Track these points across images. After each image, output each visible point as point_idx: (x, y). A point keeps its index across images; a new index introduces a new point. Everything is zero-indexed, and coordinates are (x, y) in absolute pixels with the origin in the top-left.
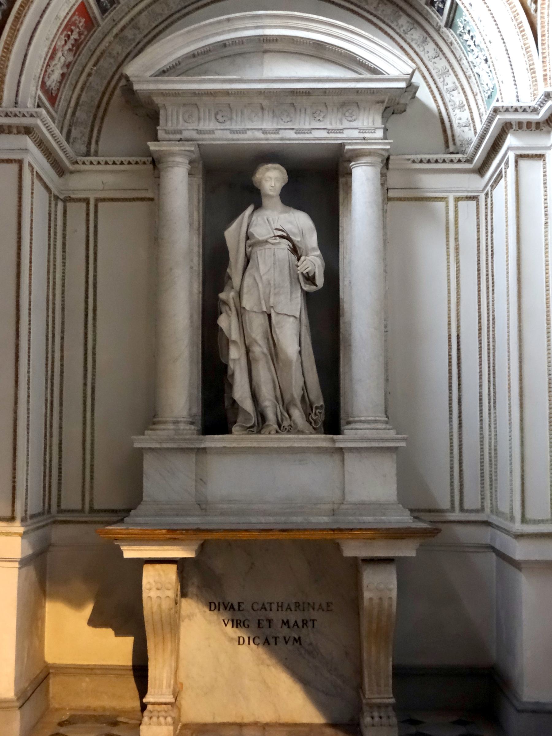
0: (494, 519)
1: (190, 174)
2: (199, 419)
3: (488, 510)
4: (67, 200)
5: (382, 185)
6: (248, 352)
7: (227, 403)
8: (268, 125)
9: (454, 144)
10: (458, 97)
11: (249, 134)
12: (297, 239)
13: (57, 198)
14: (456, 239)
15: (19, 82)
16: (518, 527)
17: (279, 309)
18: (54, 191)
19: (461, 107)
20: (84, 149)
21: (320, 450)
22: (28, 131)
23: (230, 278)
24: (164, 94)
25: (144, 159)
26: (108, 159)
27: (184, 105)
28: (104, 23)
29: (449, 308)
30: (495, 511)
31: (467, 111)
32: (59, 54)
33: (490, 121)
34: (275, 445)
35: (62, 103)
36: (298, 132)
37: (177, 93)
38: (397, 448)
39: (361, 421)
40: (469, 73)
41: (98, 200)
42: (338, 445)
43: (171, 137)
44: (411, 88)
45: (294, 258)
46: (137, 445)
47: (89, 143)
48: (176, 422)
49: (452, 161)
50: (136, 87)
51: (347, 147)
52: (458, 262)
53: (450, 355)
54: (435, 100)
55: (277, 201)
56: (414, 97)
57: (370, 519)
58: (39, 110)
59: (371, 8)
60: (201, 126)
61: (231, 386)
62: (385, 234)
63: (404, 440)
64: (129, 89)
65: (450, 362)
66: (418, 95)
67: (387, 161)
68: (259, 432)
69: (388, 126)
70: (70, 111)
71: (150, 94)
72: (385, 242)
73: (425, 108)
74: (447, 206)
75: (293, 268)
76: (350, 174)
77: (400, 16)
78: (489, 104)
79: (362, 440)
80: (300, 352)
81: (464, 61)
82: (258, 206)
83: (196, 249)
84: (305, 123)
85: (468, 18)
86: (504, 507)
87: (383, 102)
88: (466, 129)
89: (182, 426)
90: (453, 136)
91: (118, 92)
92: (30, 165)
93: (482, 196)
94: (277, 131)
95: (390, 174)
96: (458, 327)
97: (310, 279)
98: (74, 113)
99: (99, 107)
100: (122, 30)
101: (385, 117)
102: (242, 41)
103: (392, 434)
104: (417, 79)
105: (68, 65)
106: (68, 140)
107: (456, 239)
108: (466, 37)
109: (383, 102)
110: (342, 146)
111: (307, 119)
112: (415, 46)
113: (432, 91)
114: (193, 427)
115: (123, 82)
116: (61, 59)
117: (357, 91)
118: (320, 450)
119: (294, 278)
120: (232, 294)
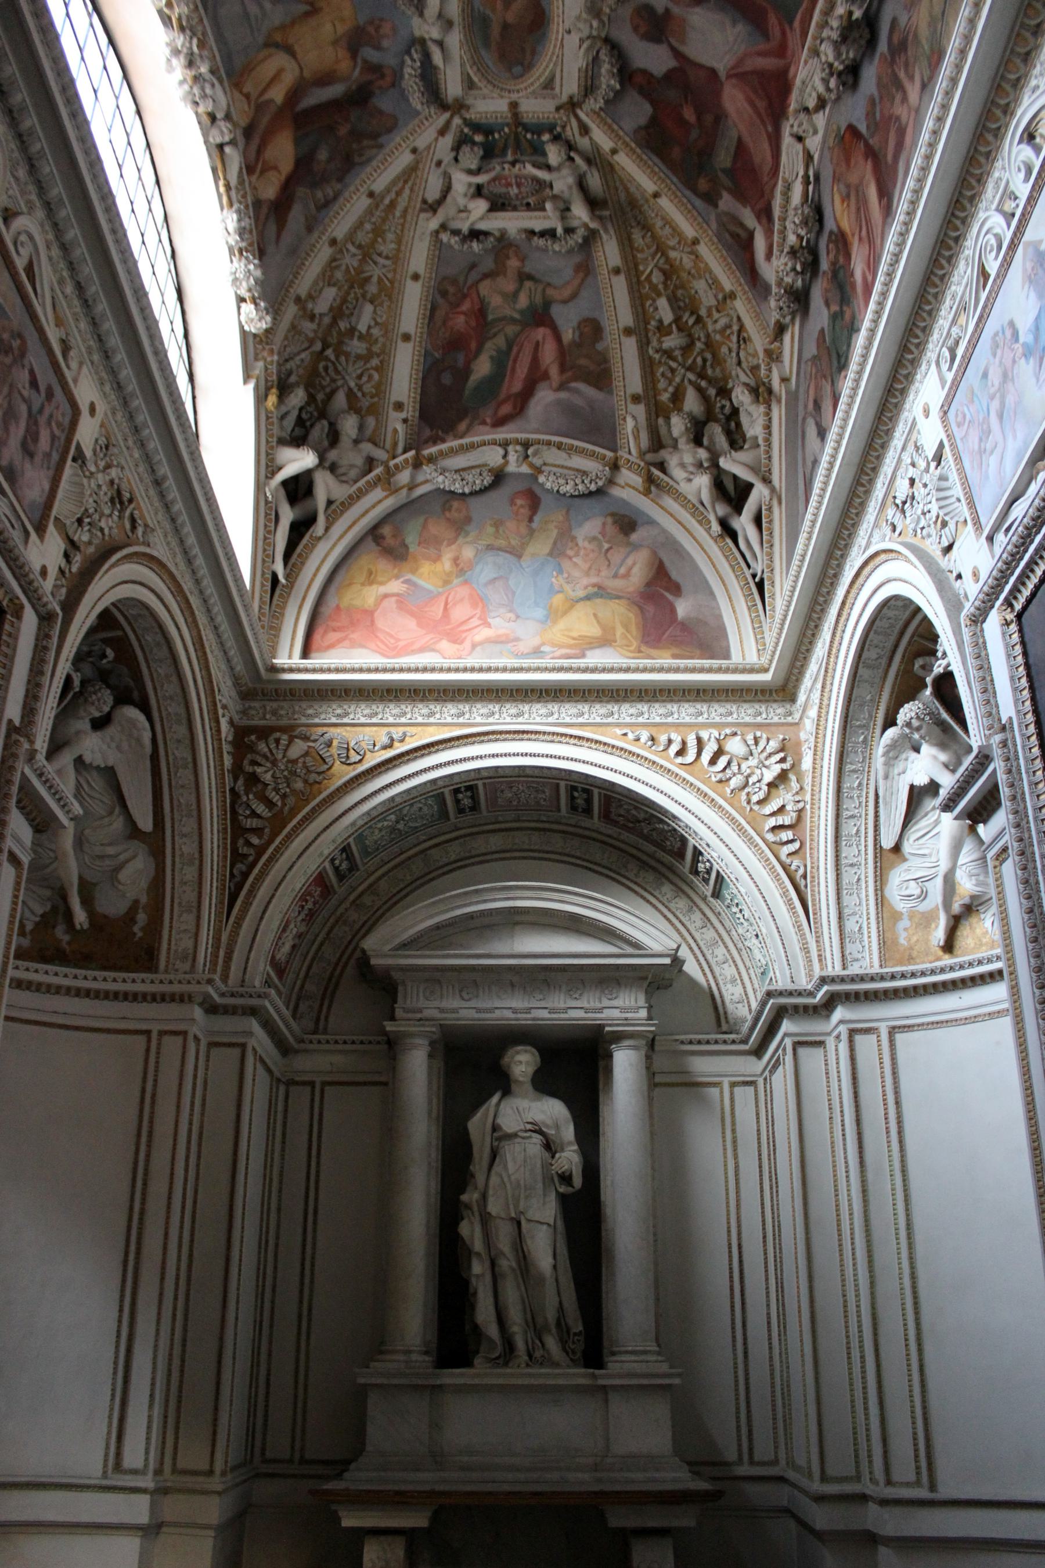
0: (791, 1475)
1: (430, 1056)
3: (783, 1462)
4: (291, 1083)
5: (648, 1068)
6: (493, 1264)
9: (727, 1022)
10: (729, 971)
11: (498, 1014)
13: (279, 1080)
14: (734, 1131)
15: (248, 959)
16: (817, 1487)
17: (530, 1215)
18: (277, 1074)
19: (733, 981)
20: (311, 1026)
22: (253, 1012)
23: (473, 1176)
25: (380, 1038)
26: (337, 1037)
27: (427, 980)
28: (341, 890)
29: (728, 1211)
30: (791, 1463)
31: (740, 986)
32: (292, 926)
33: (763, 1004)
34: (526, 1381)
35: (290, 977)
36: (552, 1011)
38: (670, 1386)
39: (627, 1352)
40: (740, 945)
41: (324, 1084)
42: (601, 1382)
43: (410, 1015)
44: (677, 962)
45: (547, 1155)
46: (361, 1381)
47: (318, 1020)
48: (408, 1352)
49: (725, 1042)
50: (373, 962)
51: (607, 1029)
52: (736, 1156)
53: (731, 1269)
54: (705, 974)
55: (529, 1087)
56: (680, 971)
57: (639, 1476)
58: (267, 990)
59: (631, 875)
60: (445, 1004)
61: (473, 1307)
62: (652, 1125)
63: (679, 1375)
64: (364, 961)
65: (731, 1277)
66: (685, 968)
67: (652, 1044)
70: (299, 983)
71: (388, 969)
72: (652, 1134)
73: (692, 982)
74: (722, 1092)
75: (546, 1166)
76: (610, 1056)
77: (662, 884)
78: (763, 981)
80: (555, 1267)
81: (734, 932)
82: (507, 1092)
83: (434, 1142)
85: (735, 891)
86: (801, 1462)
87: (645, 978)
88: (740, 1006)
89: (414, 1357)
90: (725, 1013)
91: (352, 962)
92: (254, 1049)
93: (761, 1081)
94: (528, 1010)
96: (739, 1234)
97: (566, 1178)
98: (302, 986)
99: (330, 979)
100: (360, 896)
101: (649, 995)
102: (491, 912)
103: (664, 1368)
104: (684, 953)
105: (300, 936)
106: (294, 1016)
107: (734, 1131)
108: (734, 909)
109: (646, 978)
110: (601, 1027)
111: (562, 996)
112: (680, 916)
113: (700, 964)
114: (427, 1358)
115: (358, 954)
116: (293, 930)
117: (618, 967)
118: (578, 1389)
119: (548, 1179)
120: (476, 1196)
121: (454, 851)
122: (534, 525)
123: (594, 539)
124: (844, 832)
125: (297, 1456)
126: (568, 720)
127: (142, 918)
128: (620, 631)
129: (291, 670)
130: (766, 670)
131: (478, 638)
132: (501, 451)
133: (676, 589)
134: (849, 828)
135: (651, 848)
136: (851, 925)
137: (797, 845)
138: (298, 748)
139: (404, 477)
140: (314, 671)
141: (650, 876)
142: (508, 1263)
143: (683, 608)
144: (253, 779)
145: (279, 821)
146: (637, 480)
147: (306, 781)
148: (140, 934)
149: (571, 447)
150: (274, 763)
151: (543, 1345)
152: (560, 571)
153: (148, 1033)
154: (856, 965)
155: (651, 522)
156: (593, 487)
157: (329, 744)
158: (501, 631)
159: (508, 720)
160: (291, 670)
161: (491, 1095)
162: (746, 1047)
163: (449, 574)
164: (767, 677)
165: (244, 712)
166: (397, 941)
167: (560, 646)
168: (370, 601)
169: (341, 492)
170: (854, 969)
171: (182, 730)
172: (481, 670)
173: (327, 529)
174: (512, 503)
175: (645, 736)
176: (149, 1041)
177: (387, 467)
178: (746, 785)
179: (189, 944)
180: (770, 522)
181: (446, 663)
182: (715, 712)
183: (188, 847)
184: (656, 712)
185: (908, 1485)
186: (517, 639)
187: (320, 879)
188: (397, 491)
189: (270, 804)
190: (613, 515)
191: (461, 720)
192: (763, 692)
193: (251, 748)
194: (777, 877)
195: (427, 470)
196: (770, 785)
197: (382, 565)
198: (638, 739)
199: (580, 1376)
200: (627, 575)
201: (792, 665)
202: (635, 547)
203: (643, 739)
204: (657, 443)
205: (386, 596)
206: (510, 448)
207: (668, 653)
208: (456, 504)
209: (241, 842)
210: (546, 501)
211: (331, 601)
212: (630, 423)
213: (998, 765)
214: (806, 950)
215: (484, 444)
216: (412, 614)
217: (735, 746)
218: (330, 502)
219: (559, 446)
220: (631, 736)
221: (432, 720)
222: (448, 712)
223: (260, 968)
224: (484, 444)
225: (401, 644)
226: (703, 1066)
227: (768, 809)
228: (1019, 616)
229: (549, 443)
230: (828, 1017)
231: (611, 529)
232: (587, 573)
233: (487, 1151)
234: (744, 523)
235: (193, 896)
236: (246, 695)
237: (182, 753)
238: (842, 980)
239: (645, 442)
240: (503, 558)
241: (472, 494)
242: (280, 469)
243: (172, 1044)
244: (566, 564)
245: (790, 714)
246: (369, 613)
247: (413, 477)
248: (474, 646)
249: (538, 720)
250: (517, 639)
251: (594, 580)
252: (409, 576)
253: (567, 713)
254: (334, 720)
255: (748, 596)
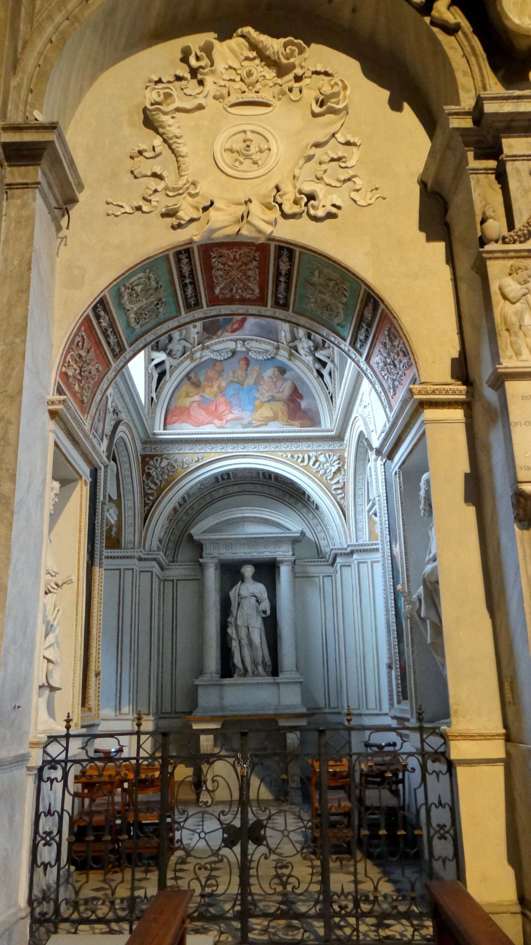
1: (216, 569)
2: (220, 671)
3: (340, 707)
6: (240, 642)
7: (231, 664)
8: (246, 551)
10: (322, 535)
11: (239, 554)
12: (258, 595)
14: (324, 593)
17: (252, 625)
19: (324, 539)
20: (171, 559)
21: (269, 684)
22: (154, 560)
23: (232, 612)
24: (204, 539)
37: (210, 539)
41: (177, 580)
44: (303, 533)
46: (196, 683)
48: (211, 673)
52: (325, 603)
59: (287, 500)
61: (233, 657)
64: (191, 536)
68: (245, 676)
69: (295, 547)
73: (309, 539)
75: (257, 608)
76: (279, 567)
79: (286, 678)
80: (261, 643)
84: (262, 550)
94: (250, 553)
95: (296, 567)
97: (265, 612)
102: (236, 518)
103: (298, 676)
106: (165, 555)
107: (324, 593)
110: (275, 558)
117: (281, 537)
118: (269, 684)
119: (258, 611)
120: (233, 619)
121: (222, 492)
122: (248, 372)
123: (270, 377)
124: (357, 493)
125: (173, 711)
126: (262, 450)
127: (114, 529)
128: (280, 414)
129: (161, 434)
130: (333, 431)
131: (228, 418)
132: (235, 343)
133: (301, 397)
134: (359, 492)
135: (292, 490)
136: (360, 526)
137: (343, 495)
138: (164, 463)
139: (198, 355)
140: (169, 434)
141: (294, 500)
142: (245, 642)
143: (304, 404)
144: (149, 475)
145: (160, 490)
146: (286, 354)
147: (168, 475)
148: (114, 535)
149: (261, 341)
150: (156, 468)
151: (257, 669)
152: (258, 391)
153: (120, 570)
154: (361, 540)
155: (292, 369)
156: (270, 357)
157: (176, 461)
158: (237, 416)
159: (240, 450)
160: (161, 434)
161: (236, 583)
162: (328, 563)
163: (217, 392)
164: (333, 433)
165: (144, 449)
166: (203, 530)
167: (259, 421)
168: (188, 404)
169: (175, 362)
170: (360, 542)
171: (127, 466)
172: (230, 433)
173: (170, 377)
174: (239, 363)
175: (289, 455)
176: (120, 572)
177: (192, 352)
178: (325, 473)
179: (132, 538)
180: (334, 376)
181: (218, 430)
182: (315, 446)
183: (130, 504)
184: (293, 447)
185: (373, 709)
186: (243, 419)
187: (175, 510)
188: (196, 360)
189: (156, 484)
190: (277, 367)
191: (223, 451)
192: (332, 438)
193: (147, 463)
194: (336, 507)
195: (206, 352)
196: (335, 473)
197: (192, 389)
198: (287, 457)
199: (270, 679)
200: (283, 392)
201: (342, 427)
202: (286, 380)
203: (289, 456)
204: (294, 338)
205: (194, 402)
206: (238, 342)
207: (297, 423)
208: (218, 364)
209: (146, 498)
210: (252, 362)
211: (173, 405)
212: (283, 334)
213: (377, 506)
214: (345, 533)
215: (228, 340)
216: (204, 409)
217: (322, 458)
218: (171, 367)
219: (257, 341)
220: (284, 455)
221: (213, 451)
222: (218, 448)
223: (155, 543)
224: (228, 340)
225: (200, 421)
226: (313, 570)
227: (333, 482)
228: (384, 464)
229: (252, 340)
230: (352, 556)
231: (277, 373)
232: (268, 391)
233: (237, 602)
234: (325, 372)
235: (132, 521)
236: (144, 443)
237: (127, 473)
238: (355, 545)
239: (289, 338)
240: (236, 386)
241: (225, 360)
242: (153, 360)
243: (129, 574)
244: (260, 388)
245: (342, 445)
246: (188, 409)
247: (201, 354)
248: (227, 421)
249: (251, 450)
250: (243, 419)
251: (271, 394)
252: (202, 394)
253: (261, 447)
254: (177, 452)
255: (327, 400)
